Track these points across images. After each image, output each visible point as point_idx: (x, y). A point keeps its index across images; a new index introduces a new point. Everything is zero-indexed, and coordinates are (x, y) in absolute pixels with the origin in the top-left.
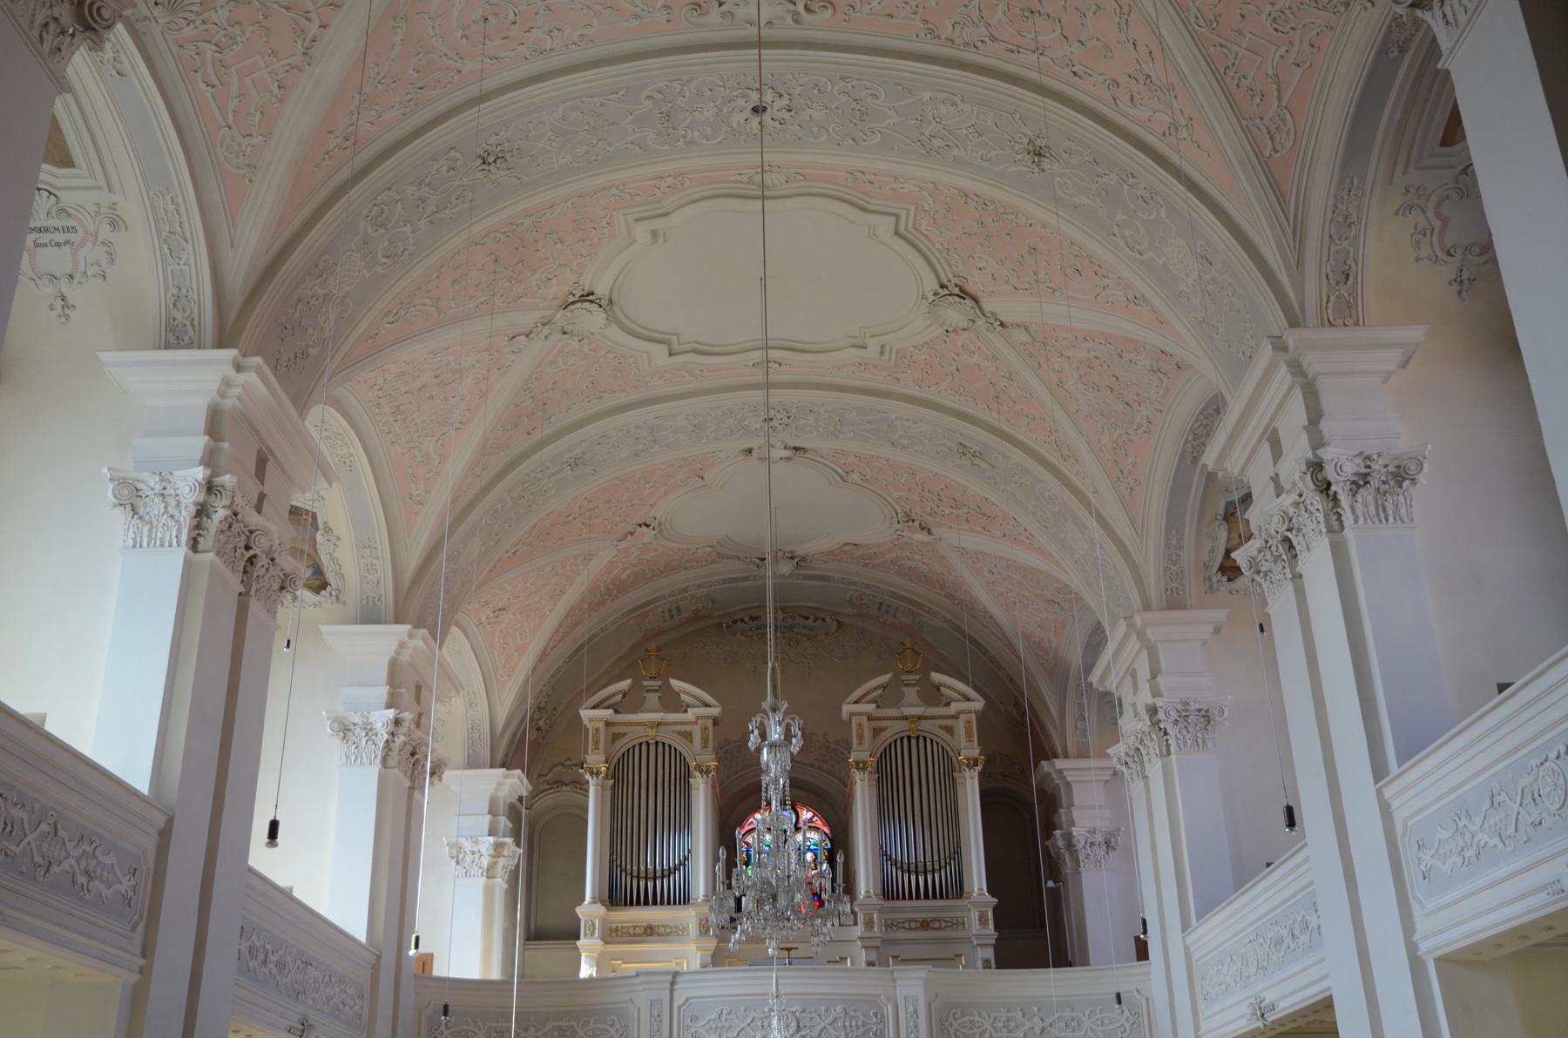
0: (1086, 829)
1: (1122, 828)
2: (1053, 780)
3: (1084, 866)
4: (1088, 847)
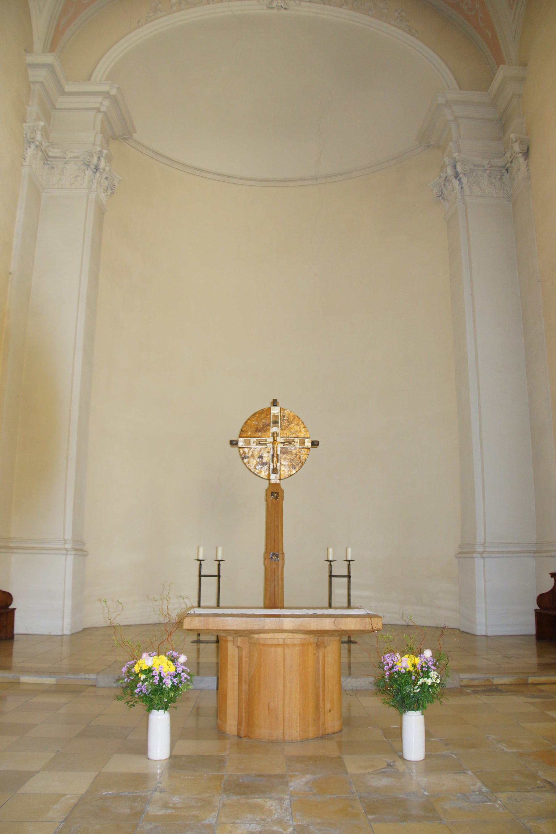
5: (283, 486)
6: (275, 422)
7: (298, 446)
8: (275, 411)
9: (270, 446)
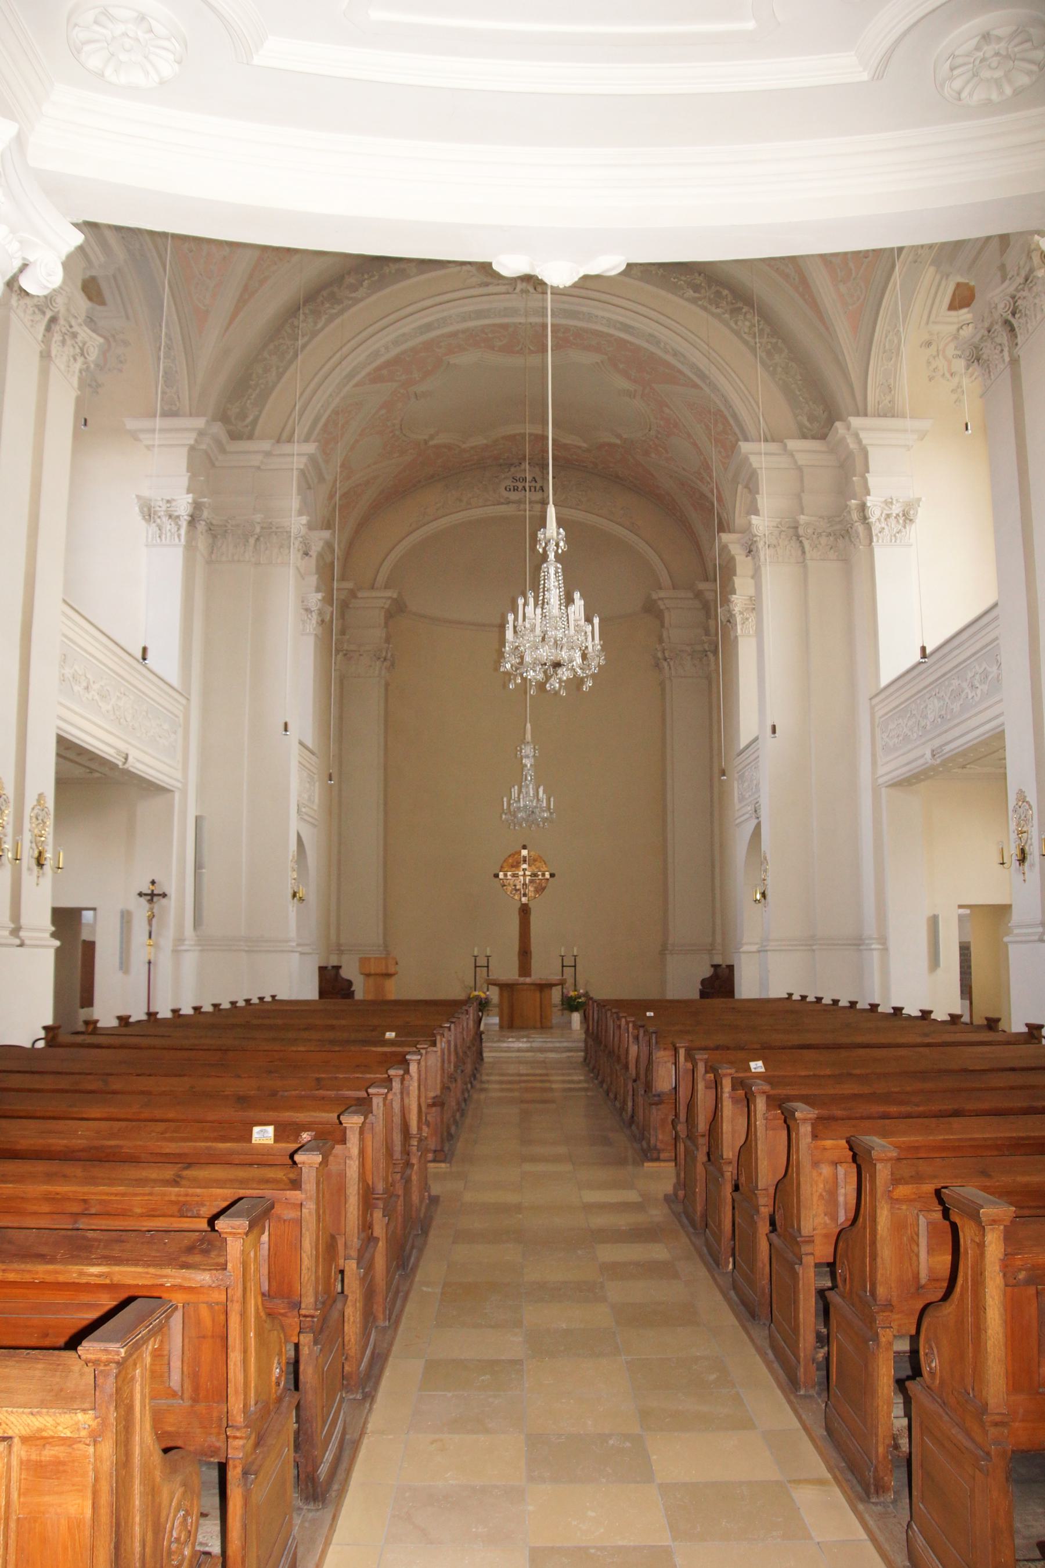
0: (883, 499)
1: (923, 499)
2: (847, 445)
3: (878, 541)
4: (882, 520)
5: (530, 905)
6: (525, 861)
7: (540, 877)
8: (524, 852)
9: (522, 878)
